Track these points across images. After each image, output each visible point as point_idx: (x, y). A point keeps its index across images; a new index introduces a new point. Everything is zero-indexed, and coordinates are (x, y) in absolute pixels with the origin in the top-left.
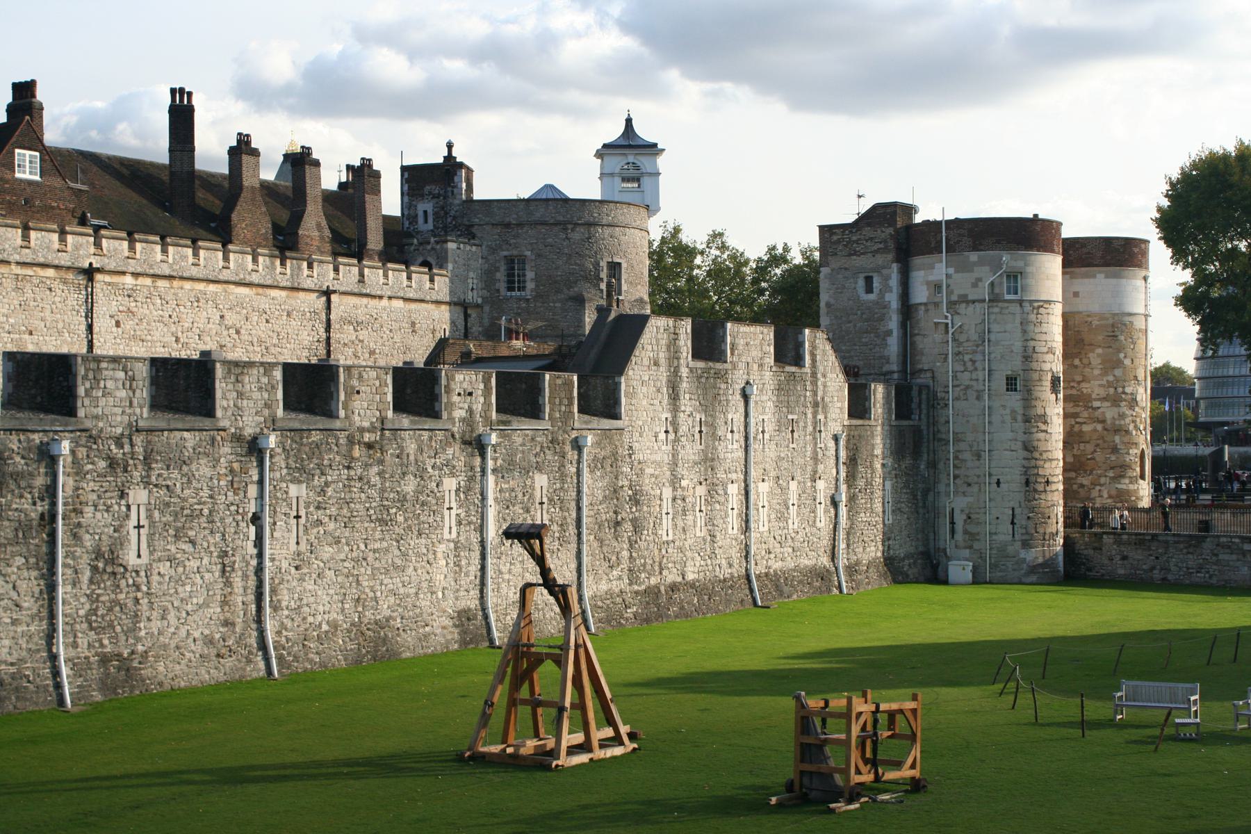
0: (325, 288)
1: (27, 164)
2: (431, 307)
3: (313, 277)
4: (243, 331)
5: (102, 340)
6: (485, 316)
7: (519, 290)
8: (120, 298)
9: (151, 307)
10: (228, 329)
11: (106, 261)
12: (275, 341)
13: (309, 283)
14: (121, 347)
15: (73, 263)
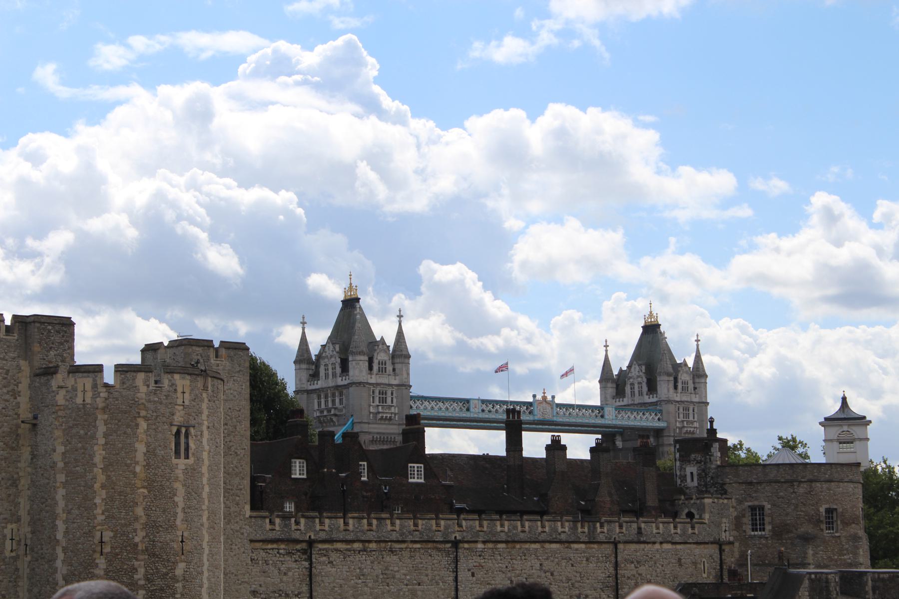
0: (612, 540)
1: (416, 473)
2: (695, 546)
3: (604, 533)
4: (555, 573)
5: (463, 586)
6: (736, 550)
7: (760, 531)
8: (474, 558)
9: (494, 561)
10: (545, 573)
11: (465, 534)
12: (578, 579)
13: (602, 538)
14: (475, 589)
15: (445, 538)
